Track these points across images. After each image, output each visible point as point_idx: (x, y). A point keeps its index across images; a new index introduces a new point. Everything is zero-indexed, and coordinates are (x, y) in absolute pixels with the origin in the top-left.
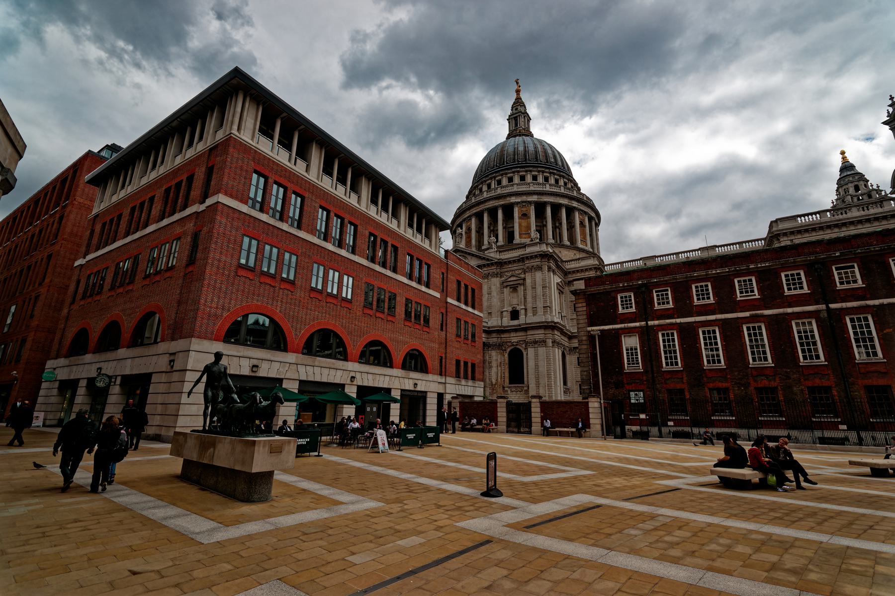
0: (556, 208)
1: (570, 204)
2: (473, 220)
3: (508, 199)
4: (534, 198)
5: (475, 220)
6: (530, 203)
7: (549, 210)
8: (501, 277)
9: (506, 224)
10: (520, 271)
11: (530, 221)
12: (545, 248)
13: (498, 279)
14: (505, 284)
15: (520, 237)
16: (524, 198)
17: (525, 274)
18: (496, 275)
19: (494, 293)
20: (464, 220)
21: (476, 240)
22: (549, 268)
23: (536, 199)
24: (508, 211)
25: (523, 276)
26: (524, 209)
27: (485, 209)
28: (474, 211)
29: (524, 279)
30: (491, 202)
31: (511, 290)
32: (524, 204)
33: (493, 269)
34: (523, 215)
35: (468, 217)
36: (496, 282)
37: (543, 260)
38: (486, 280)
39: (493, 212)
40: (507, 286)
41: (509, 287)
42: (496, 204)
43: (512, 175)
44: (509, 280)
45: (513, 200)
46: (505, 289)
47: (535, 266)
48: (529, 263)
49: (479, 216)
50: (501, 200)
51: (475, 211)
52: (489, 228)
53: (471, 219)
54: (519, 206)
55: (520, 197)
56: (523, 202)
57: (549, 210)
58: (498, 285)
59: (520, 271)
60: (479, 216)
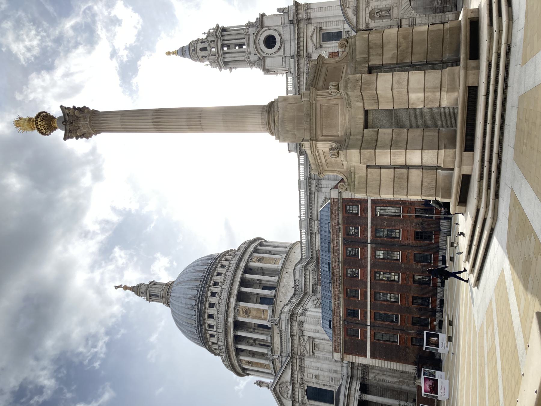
0: (244, 283)
1: (242, 269)
3: (229, 324)
4: (233, 300)
5: (243, 356)
6: (236, 305)
7: (245, 289)
8: (304, 356)
9: (251, 328)
10: (302, 339)
11: (253, 308)
12: (285, 315)
13: (306, 359)
14: (311, 353)
16: (231, 310)
17: (304, 336)
18: (302, 360)
19: (318, 365)
20: (240, 366)
22: (303, 314)
23: (234, 299)
24: (238, 325)
25: (306, 338)
26: (241, 311)
27: (235, 346)
28: (233, 356)
29: (309, 337)
30: (229, 340)
31: (316, 348)
32: (236, 311)
33: (296, 362)
34: (246, 314)
35: (238, 362)
36: (308, 362)
37: (295, 319)
38: (305, 369)
39: (238, 339)
40: (313, 353)
41: (314, 351)
42: (232, 335)
43: (206, 315)
44: (308, 349)
45: (231, 320)
46: (316, 354)
47: (300, 327)
48: (296, 331)
49: (239, 351)
50: (229, 331)
51: (234, 355)
52: (252, 345)
53: (241, 360)
54: (237, 316)
56: (234, 312)
57: (245, 289)
58: (312, 360)
59: (302, 339)
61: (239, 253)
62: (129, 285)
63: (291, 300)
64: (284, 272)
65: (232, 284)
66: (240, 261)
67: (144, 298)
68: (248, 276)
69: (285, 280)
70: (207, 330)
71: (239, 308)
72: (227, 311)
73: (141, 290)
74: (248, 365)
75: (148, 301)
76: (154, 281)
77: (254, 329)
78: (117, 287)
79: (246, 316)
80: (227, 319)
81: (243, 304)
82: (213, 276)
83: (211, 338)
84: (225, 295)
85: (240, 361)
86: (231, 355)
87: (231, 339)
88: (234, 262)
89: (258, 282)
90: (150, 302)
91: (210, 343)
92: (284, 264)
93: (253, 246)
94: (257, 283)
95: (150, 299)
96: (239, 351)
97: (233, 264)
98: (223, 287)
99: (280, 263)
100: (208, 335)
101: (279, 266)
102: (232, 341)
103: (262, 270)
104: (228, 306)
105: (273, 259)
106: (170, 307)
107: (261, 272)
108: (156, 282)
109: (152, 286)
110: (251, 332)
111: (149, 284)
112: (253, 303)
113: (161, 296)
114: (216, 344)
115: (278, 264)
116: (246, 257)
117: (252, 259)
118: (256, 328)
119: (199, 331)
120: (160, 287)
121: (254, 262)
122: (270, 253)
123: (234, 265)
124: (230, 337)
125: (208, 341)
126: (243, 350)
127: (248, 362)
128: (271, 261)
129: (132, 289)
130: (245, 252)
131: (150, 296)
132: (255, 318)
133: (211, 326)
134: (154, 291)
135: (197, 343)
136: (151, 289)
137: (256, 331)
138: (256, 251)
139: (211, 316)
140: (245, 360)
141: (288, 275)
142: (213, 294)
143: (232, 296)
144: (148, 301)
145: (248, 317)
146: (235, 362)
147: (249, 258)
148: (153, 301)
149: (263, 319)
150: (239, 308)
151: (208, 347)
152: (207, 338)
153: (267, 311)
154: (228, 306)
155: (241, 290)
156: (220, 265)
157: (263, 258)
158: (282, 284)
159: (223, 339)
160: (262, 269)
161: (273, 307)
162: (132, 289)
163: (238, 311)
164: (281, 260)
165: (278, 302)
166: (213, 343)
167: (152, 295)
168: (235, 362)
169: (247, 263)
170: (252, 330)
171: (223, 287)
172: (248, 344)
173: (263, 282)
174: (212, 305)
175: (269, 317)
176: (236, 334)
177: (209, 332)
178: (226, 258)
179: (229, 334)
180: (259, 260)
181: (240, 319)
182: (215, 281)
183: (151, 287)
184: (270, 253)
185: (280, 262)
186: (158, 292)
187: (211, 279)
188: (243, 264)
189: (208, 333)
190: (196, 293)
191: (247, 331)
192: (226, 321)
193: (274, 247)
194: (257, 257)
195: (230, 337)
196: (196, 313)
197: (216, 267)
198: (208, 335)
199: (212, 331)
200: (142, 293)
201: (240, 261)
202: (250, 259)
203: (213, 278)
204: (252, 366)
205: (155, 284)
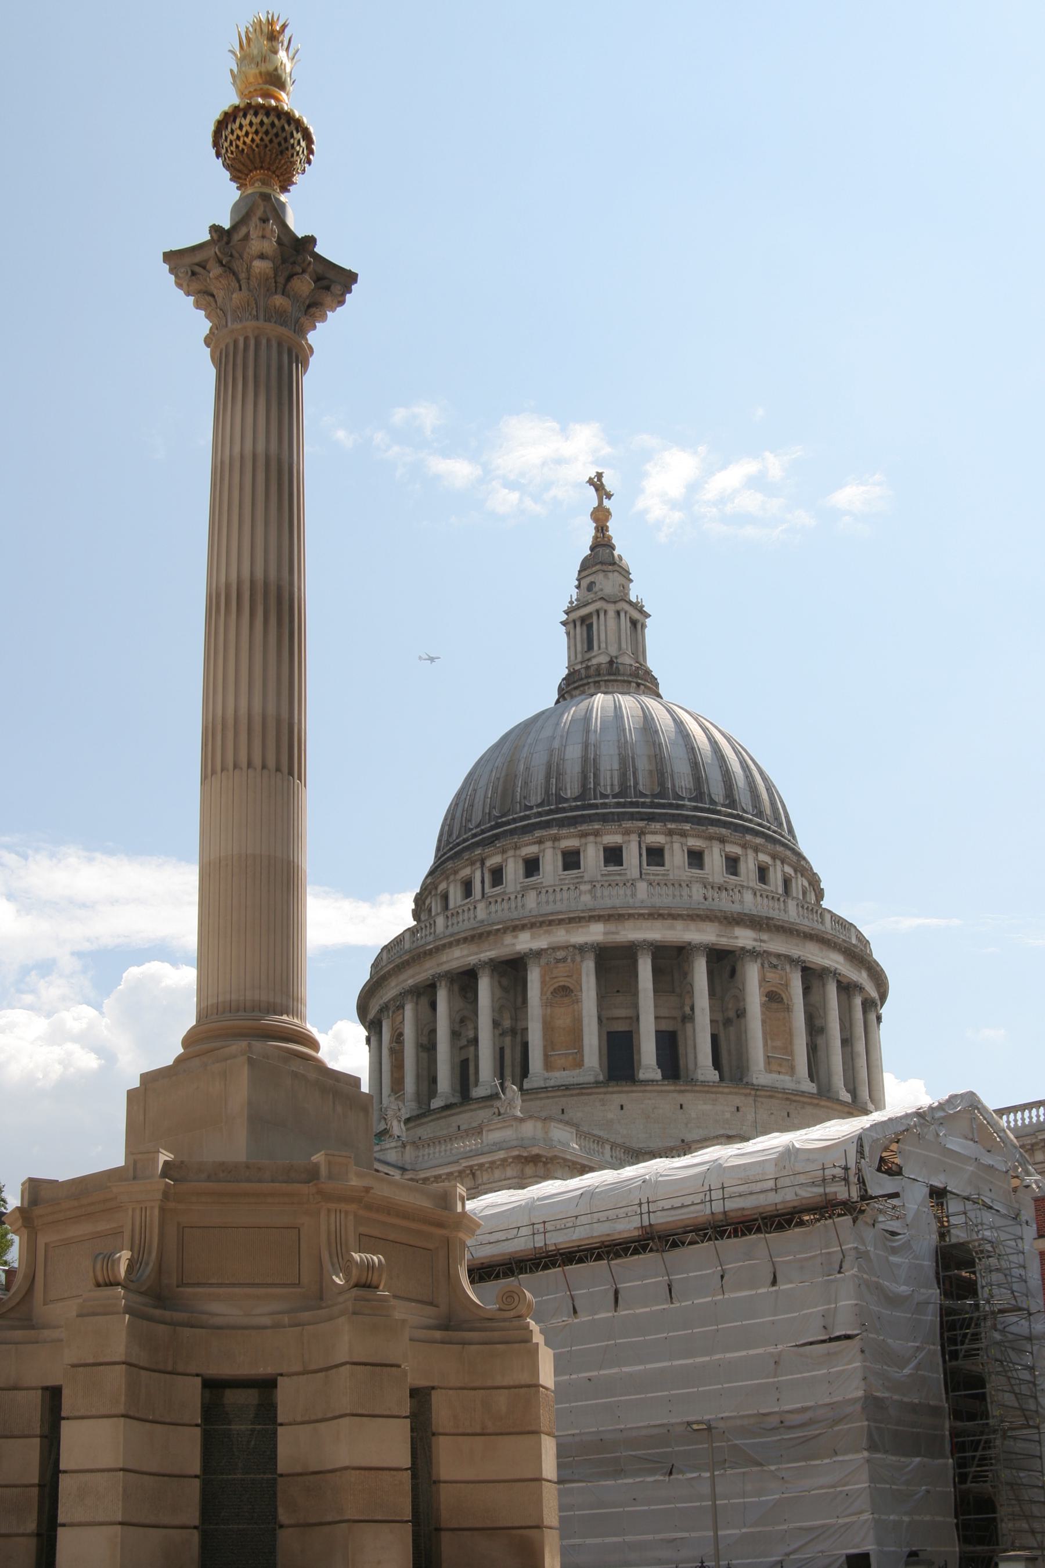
2: (409, 1010)
3: (508, 939)
4: (595, 933)
5: (416, 1011)
6: (581, 949)
15: (548, 1065)
16: (561, 936)
21: (418, 1077)
27: (440, 976)
28: (412, 977)
34: (555, 992)
35: (393, 999)
42: (473, 960)
45: (524, 942)
53: (401, 1007)
54: (543, 961)
55: (548, 932)
56: (554, 949)
60: (427, 991)
61: (792, 913)
62: (614, 528)
63: (608, 1147)
64: (738, 1101)
65: (656, 915)
66: (756, 923)
67: (574, 597)
68: (700, 971)
69: (707, 1107)
70: (483, 864)
71: (573, 961)
72: (551, 923)
73: (599, 578)
74: (392, 1036)
75: (564, 617)
76: (648, 616)
77: (513, 1032)
78: (597, 484)
79: (549, 993)
80: (523, 927)
81: (588, 975)
82: (683, 834)
83: (459, 885)
84: (614, 898)
85: (397, 1006)
86: (410, 972)
87: (459, 957)
88: (749, 903)
89: (687, 1009)
90: (564, 623)
91: (442, 886)
92: (771, 1092)
93: (834, 960)
94: (682, 1007)
95: (574, 622)
96: (427, 991)
97: (742, 902)
98: (642, 886)
99: (775, 1076)
100: (467, 871)
101: (759, 1073)
102: (454, 965)
103: (738, 1016)
104: (571, 920)
105: (788, 1048)
106: (558, 702)
107: (731, 1014)
108: (643, 626)
109: (622, 615)
110: (496, 1024)
111: (630, 603)
112: (600, 1007)
113: (589, 660)
114: (446, 907)
115: (771, 1072)
116: (777, 945)
117: (775, 967)
118: (519, 1039)
119: (475, 836)
120: (624, 646)
121: (763, 980)
122: (815, 1029)
123: (736, 908)
124: (465, 952)
125: (447, 878)
126: (433, 1006)
127: (401, 1034)
128: (778, 1043)
129: (602, 544)
130: (798, 935)
131: (583, 619)
132: (548, 1028)
133: (497, 876)
134: (602, 628)
135: (440, 841)
136: (611, 614)
137: (508, 1040)
138: (812, 976)
139: (532, 866)
140: (402, 1022)
141: (728, 1115)
142: (613, 856)
143: (612, 927)
144: (564, 617)
145: (547, 1004)
146: (390, 992)
147: (778, 956)
148: (568, 634)
149: (546, 1056)
150: (573, 961)
151: (429, 881)
152: (456, 873)
153: (579, 1064)
154: (571, 920)
155: (639, 953)
156: (734, 849)
157: (788, 1009)
158: (687, 1098)
159: (456, 929)
160: (741, 1014)
161: (597, 1084)
162: (602, 544)
163: (558, 961)
164: (787, 1078)
165: (617, 1099)
166: (445, 897)
167: (590, 627)
168: (390, 992)
169: (754, 954)
170: (507, 1023)
171: (642, 886)
172: (458, 1020)
173: (689, 1026)
174: (571, 860)
175: (560, 1077)
176: (480, 974)
177: (478, 875)
178: (771, 869)
179: (473, 948)
180: (774, 999)
181: (534, 977)
182: (667, 847)
183: (618, 613)
184: (815, 1029)
185: (782, 1077)
186: (603, 645)
187: (670, 833)
188: (744, 938)
189: (473, 872)
190: (609, 791)
191: (498, 1010)
192: (517, 928)
193: (847, 1042)
194: (787, 986)
195: (465, 952)
196: (535, 810)
197: (722, 840)
198: (467, 871)
199: (483, 882)
200: (590, 587)
201: (756, 923)
202: (775, 961)
203: (675, 838)
204: (392, 1051)
205: (634, 623)
